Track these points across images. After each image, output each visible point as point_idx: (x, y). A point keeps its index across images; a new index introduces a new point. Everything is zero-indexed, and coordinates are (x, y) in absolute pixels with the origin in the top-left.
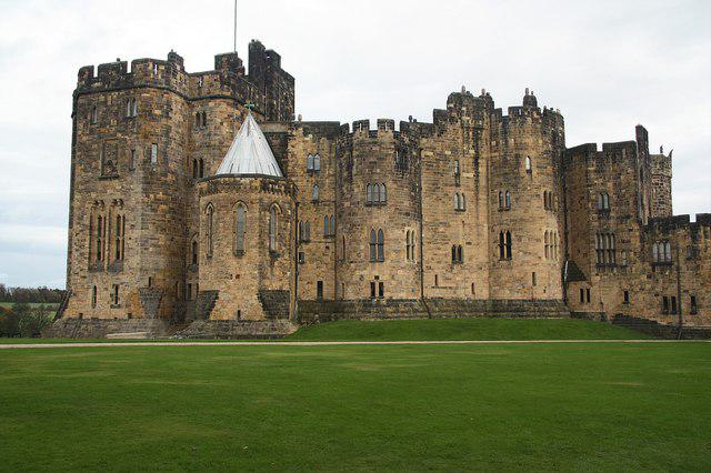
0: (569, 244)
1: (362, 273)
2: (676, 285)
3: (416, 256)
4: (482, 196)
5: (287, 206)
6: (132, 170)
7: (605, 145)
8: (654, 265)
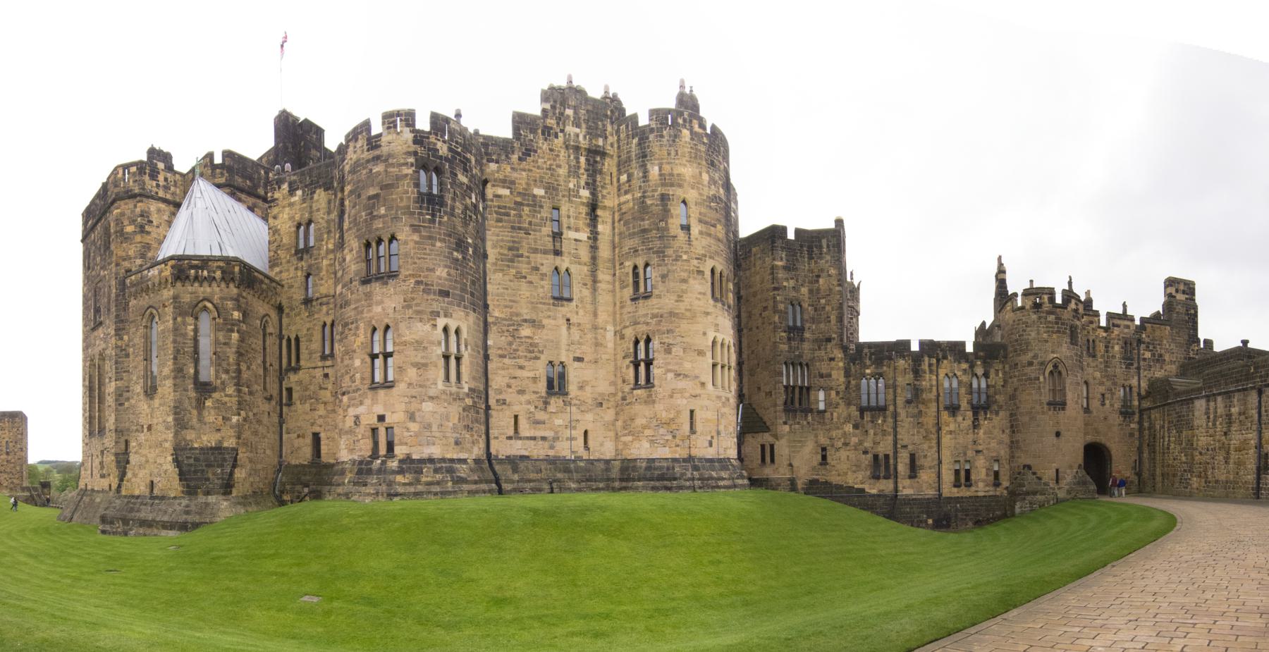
5: (230, 304)
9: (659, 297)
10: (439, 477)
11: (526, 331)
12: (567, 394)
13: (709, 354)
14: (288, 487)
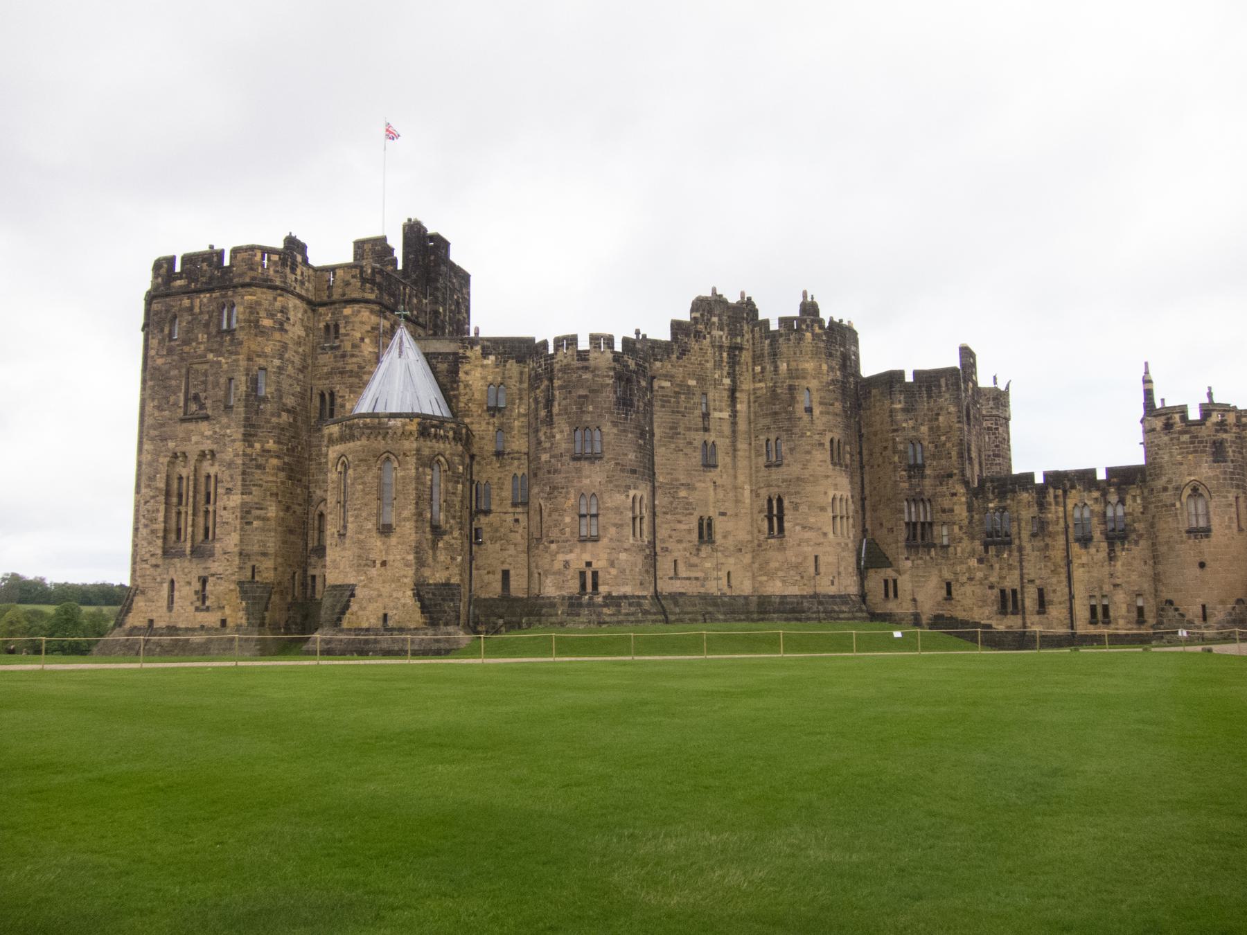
0: (868, 514)
1: (568, 557)
2: (1017, 572)
3: (646, 533)
4: (742, 445)
6: (228, 408)
7: (917, 374)
8: (986, 546)
9: (788, 465)
10: (632, 609)
11: (683, 493)
12: (714, 542)
13: (830, 510)
14: (482, 619)
